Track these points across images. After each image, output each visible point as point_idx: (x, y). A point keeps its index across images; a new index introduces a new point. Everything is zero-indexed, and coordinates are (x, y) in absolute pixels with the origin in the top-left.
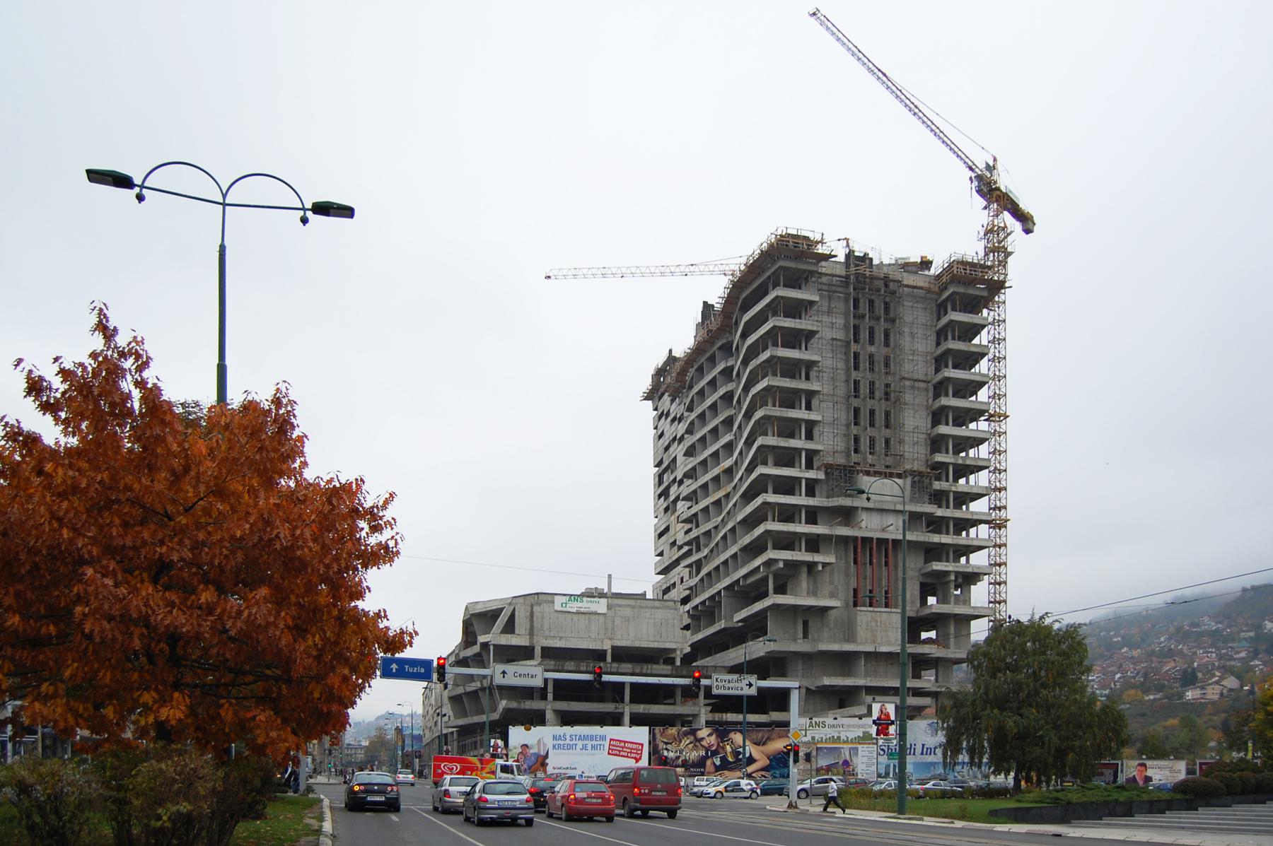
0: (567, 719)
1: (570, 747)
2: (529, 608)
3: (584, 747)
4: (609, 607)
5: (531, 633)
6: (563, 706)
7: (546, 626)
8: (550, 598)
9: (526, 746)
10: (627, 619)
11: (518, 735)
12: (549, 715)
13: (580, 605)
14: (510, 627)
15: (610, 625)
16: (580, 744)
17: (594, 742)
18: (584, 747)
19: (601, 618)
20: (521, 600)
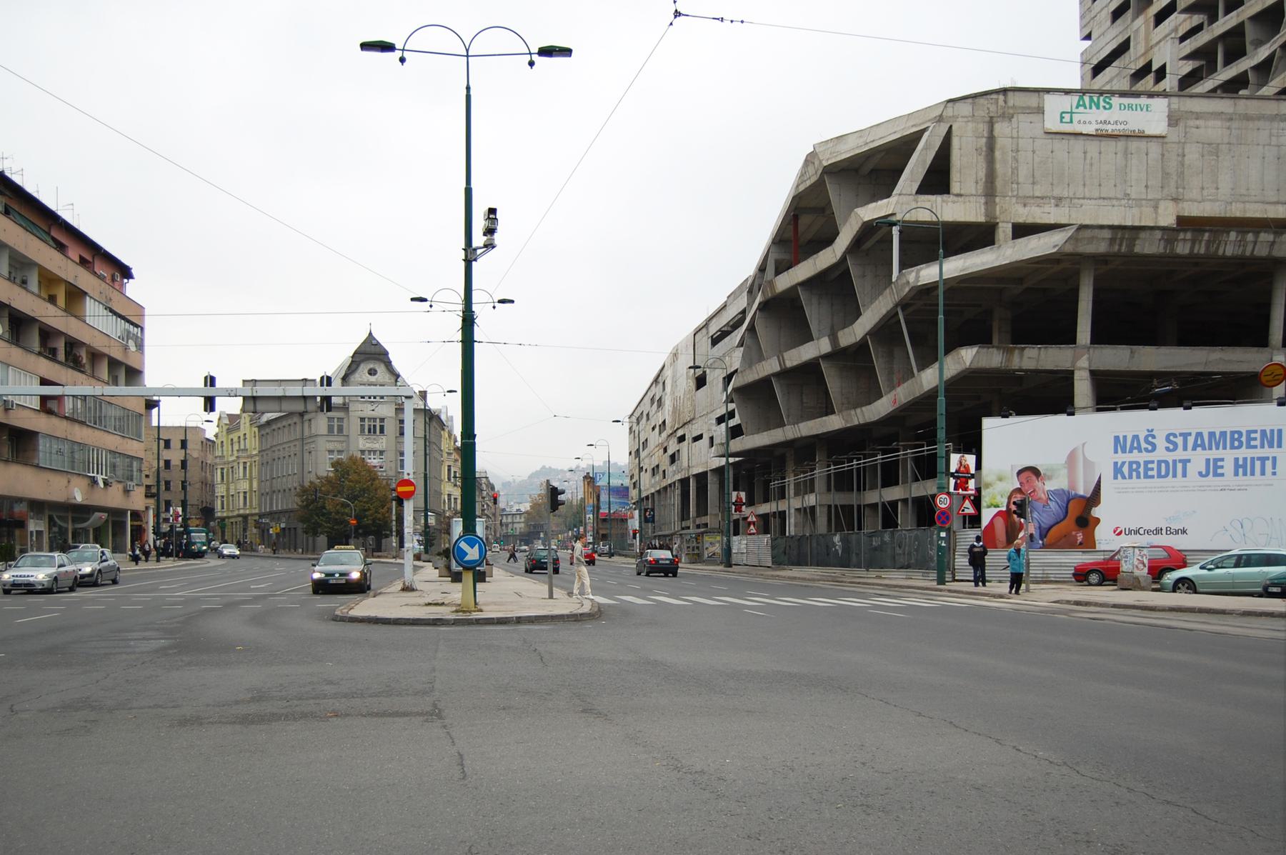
0: (1116, 393)
1: (1167, 470)
2: (983, 128)
3: (1214, 468)
4: (1173, 120)
5: (990, 191)
6: (1118, 358)
7: (1023, 172)
8: (1032, 100)
9: (1034, 471)
10: (1213, 149)
11: (1010, 444)
12: (1083, 389)
13: (1103, 115)
14: (937, 180)
15: (1173, 165)
16: (1198, 459)
17: (1244, 453)
18: (1214, 468)
19: (1154, 148)
20: (965, 109)
